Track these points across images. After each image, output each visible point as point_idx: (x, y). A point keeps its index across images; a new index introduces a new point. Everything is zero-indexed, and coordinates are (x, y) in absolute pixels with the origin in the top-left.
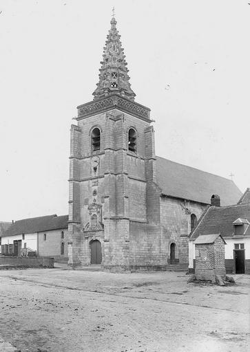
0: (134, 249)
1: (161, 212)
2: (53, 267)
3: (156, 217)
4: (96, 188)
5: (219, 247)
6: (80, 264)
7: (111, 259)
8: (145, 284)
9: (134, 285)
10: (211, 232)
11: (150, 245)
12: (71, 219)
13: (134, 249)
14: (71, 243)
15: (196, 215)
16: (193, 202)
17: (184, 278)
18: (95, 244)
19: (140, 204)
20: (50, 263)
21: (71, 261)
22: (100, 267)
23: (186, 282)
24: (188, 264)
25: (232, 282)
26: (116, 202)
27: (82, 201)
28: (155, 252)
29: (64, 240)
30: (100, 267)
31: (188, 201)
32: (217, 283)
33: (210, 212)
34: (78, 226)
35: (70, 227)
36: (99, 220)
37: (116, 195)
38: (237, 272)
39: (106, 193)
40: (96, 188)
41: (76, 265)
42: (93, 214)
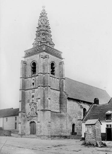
0: (53, 127)
1: (67, 107)
2: (11, 136)
3: (65, 109)
4: (33, 94)
5: (98, 126)
6: (24, 134)
7: (41, 132)
8: (59, 146)
9: (53, 146)
10: (94, 117)
11: (61, 125)
12: (20, 110)
13: (53, 127)
14: (20, 123)
15: (86, 109)
16: (84, 102)
17: (79, 143)
18: (32, 124)
19: (57, 103)
20: (9, 133)
21: (20, 133)
22: (35, 136)
23: (80, 145)
24: (82, 135)
25: (105, 145)
26: (44, 101)
27: (26, 101)
28: (64, 128)
29: (17, 121)
30: (35, 136)
31: (82, 101)
32: (97, 146)
33: (93, 107)
34: (24, 114)
35: (20, 114)
36: (35, 111)
37: (44, 98)
38: (108, 140)
39: (39, 97)
40: (33, 94)
41: (23, 135)
42: (32, 107)
